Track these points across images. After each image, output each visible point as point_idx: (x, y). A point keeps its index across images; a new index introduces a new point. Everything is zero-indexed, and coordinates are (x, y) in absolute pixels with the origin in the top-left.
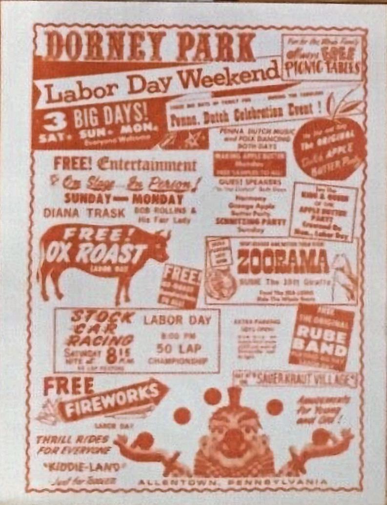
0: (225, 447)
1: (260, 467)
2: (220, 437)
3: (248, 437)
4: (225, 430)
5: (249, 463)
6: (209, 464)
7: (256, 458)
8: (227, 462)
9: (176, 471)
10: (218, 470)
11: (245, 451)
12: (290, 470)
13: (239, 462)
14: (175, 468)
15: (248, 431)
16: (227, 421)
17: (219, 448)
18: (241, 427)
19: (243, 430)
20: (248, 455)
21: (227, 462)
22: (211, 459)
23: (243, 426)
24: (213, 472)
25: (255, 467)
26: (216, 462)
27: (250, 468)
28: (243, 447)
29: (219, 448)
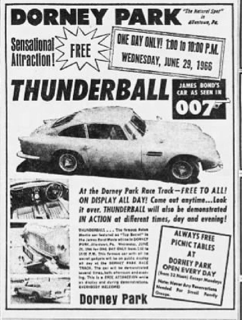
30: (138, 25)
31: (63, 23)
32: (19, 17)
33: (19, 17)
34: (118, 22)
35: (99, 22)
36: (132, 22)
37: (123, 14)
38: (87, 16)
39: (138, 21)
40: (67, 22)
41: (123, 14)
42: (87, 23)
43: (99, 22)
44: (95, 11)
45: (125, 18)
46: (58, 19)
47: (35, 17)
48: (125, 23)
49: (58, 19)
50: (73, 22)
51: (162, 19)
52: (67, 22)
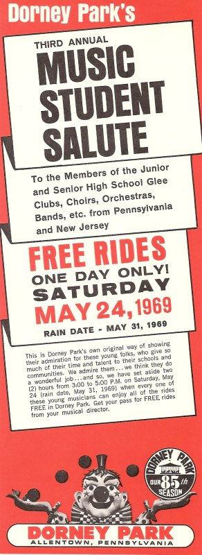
0: (94, 500)
1: (121, 516)
2: (91, 493)
3: (112, 493)
4: (95, 487)
5: (113, 513)
6: (82, 513)
7: (118, 509)
8: (97, 512)
9: (57, 519)
10: (89, 517)
11: (109, 505)
12: (145, 518)
13: (105, 512)
14: (56, 516)
15: (112, 488)
16: (97, 481)
17: (90, 500)
18: (107, 485)
19: (108, 488)
20: (112, 507)
21: (97, 512)
22: (84, 509)
23: (107, 485)
24: (85, 519)
25: (117, 516)
26: (87, 512)
27: (114, 516)
28: (108, 500)
29: (90, 500)
30: (137, 539)
31: (72, 537)
32: (35, 533)
33: (35, 533)
34: (121, 536)
35: (103, 536)
36: (132, 537)
37: (124, 531)
38: (92, 533)
39: (137, 536)
40: (75, 537)
41: (124, 531)
42: (92, 538)
43: (103, 536)
44: (99, 529)
45: (127, 534)
46: (68, 535)
47: (48, 533)
48: (126, 538)
49: (68, 535)
50: (80, 537)
51: (158, 535)
52: (75, 537)
